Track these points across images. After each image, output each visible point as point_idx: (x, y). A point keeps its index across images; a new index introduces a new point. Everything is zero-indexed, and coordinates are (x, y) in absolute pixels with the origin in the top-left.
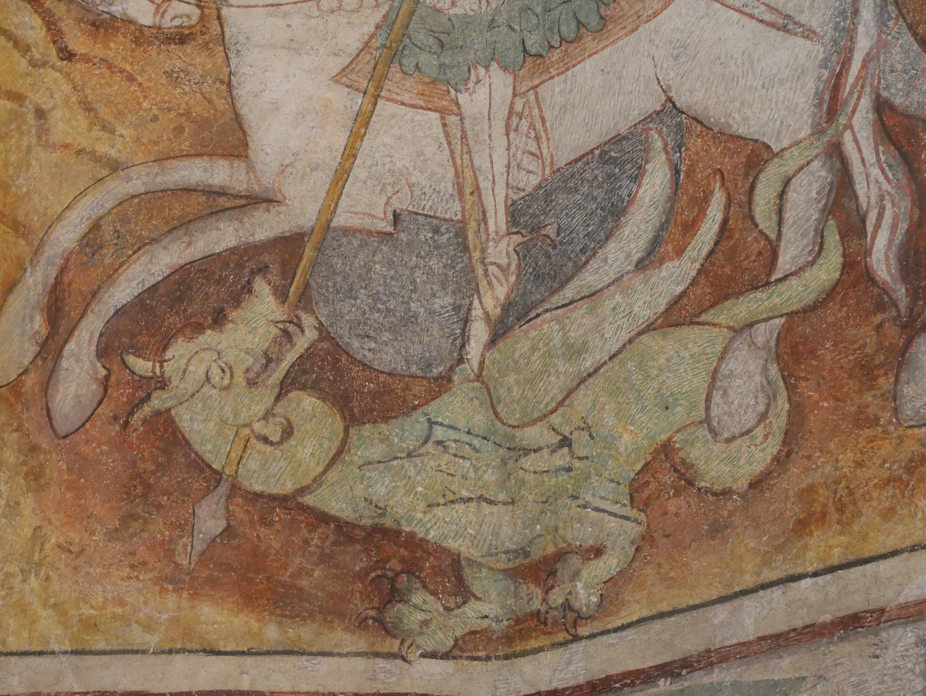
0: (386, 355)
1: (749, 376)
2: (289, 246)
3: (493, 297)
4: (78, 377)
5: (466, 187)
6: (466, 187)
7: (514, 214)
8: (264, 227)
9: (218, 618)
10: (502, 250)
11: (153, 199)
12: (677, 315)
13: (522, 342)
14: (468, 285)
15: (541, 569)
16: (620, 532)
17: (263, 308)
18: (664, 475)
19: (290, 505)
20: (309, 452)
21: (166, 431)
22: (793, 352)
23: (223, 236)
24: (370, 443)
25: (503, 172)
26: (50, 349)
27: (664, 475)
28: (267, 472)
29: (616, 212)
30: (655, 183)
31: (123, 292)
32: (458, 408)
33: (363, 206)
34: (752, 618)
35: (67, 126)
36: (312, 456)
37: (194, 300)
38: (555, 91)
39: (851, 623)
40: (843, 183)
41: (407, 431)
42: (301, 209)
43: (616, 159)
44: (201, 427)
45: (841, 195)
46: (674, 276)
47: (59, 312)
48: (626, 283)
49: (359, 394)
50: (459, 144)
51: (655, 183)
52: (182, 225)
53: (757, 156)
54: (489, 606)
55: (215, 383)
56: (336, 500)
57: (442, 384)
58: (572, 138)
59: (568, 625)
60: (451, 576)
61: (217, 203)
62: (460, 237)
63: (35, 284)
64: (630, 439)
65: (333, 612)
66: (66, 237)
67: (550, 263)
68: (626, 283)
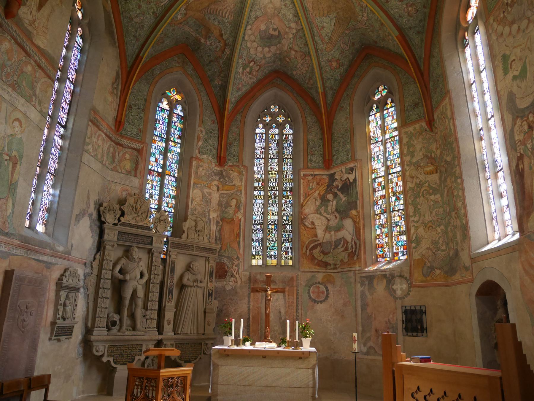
0: (326, 251)
1: (347, 256)
2: (320, 244)
3: (333, 247)
4: (308, 253)
5: (331, 239)
6: (331, 239)
7: (334, 242)
8: (319, 242)
9: (317, 267)
10: (333, 244)
11: (312, 240)
12: (343, 251)
13: (334, 251)
14: (331, 246)
15: (335, 265)
16: (340, 263)
17: (319, 248)
18: (342, 261)
19: (321, 261)
20: (322, 257)
21: (313, 256)
22: (349, 255)
23: (316, 243)
24: (325, 257)
25: (334, 239)
26: (306, 251)
27: (342, 261)
28: (319, 258)
29: (340, 243)
30: (342, 242)
31: (310, 247)
32: (331, 254)
33: (325, 241)
34: (346, 270)
35: (306, 235)
36: (321, 257)
37: (315, 247)
38: (337, 234)
39: (350, 271)
40: (352, 246)
41: (327, 256)
42: (321, 241)
43: (340, 240)
44: (315, 256)
45: (352, 246)
46: (343, 249)
47: (307, 248)
48: (340, 249)
49: (325, 253)
50: (331, 236)
51: (342, 242)
52: (314, 242)
53: (348, 242)
54: (332, 267)
55: (316, 252)
56: (323, 260)
57: (329, 253)
58: (338, 238)
59: (336, 268)
60: (330, 265)
61: (316, 241)
62: (331, 243)
63: (305, 246)
64: (340, 258)
65: (323, 267)
66: (307, 243)
67: (336, 246)
68: (340, 249)
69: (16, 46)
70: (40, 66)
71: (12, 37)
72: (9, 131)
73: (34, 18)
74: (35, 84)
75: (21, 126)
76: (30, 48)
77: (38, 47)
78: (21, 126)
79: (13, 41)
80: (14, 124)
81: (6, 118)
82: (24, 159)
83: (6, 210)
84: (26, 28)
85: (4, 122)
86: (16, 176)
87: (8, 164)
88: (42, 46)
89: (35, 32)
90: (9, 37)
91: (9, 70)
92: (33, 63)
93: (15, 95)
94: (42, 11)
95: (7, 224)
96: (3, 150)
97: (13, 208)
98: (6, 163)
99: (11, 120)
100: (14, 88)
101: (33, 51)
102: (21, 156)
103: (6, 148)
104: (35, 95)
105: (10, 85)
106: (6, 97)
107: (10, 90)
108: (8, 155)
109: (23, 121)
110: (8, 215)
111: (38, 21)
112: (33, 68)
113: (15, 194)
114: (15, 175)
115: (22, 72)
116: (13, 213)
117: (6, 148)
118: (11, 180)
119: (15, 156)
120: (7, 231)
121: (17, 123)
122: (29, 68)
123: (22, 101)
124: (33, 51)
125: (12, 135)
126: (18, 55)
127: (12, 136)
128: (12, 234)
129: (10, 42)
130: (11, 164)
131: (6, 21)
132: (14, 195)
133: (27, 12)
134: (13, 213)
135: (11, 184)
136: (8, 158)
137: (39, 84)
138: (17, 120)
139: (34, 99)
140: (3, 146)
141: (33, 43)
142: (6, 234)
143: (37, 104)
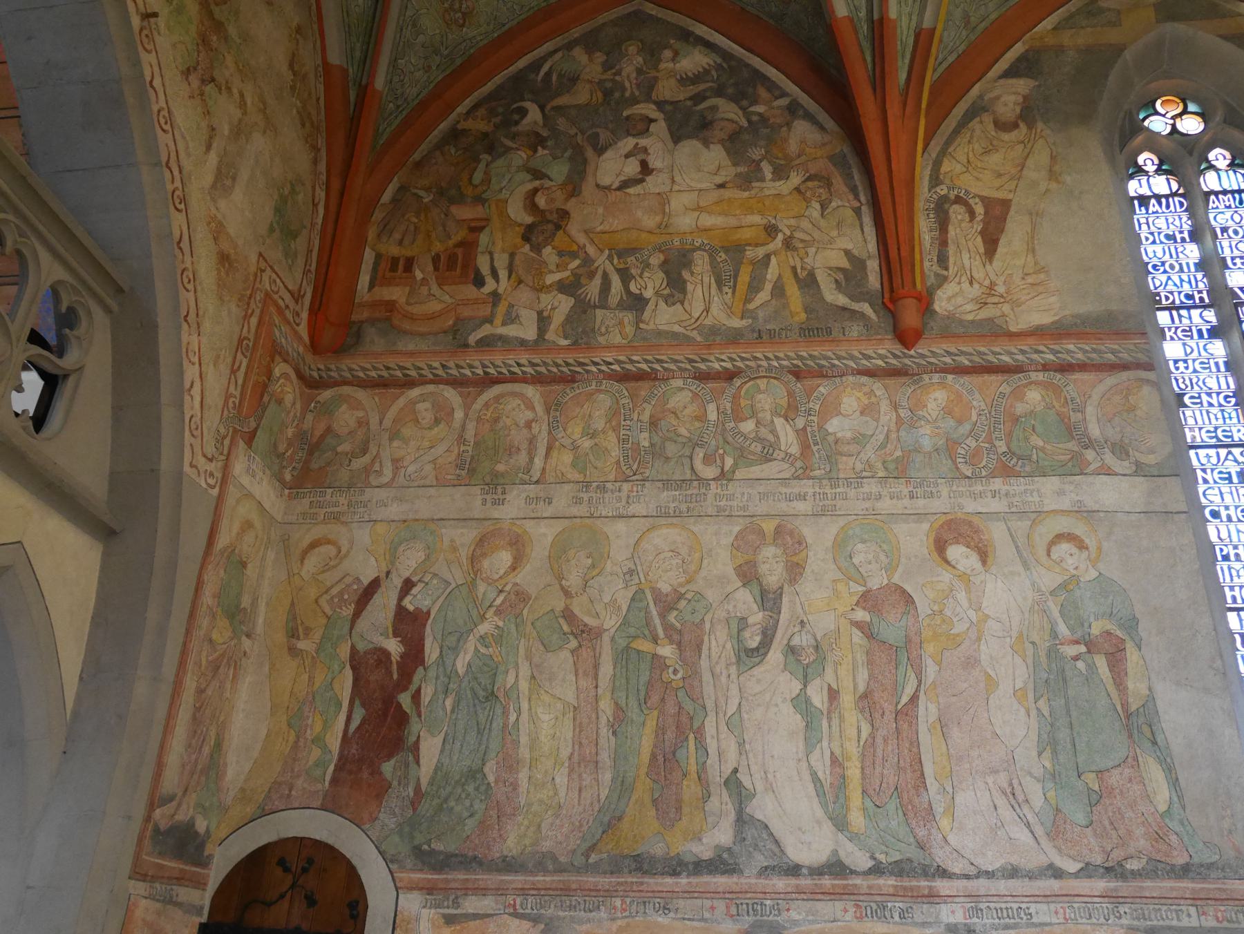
69: (965, 379)
70: (1065, 368)
71: (945, 370)
72: (1049, 580)
73: (987, 283)
74: (1075, 417)
75: (1082, 546)
76: (1010, 354)
77: (1038, 332)
78: (1082, 546)
79: (950, 377)
80: (1054, 556)
81: (1021, 556)
82: (1144, 628)
83: (1148, 797)
84: (973, 322)
85: (1020, 568)
86: (1136, 686)
87: (1092, 667)
88: (1046, 319)
89: (1006, 308)
90: (936, 378)
91: (973, 444)
92: (1040, 376)
93: (1017, 486)
94: (1001, 249)
95: (1174, 838)
96: (1054, 634)
97: (1174, 783)
98: (1080, 665)
99: (1041, 552)
100: (1007, 472)
101: (1023, 352)
102: (1131, 624)
103: (1063, 629)
104: (1089, 444)
105: (992, 475)
106: (996, 506)
107: (997, 484)
108: (1077, 642)
109: (1080, 530)
110: (1162, 808)
111: (1000, 281)
112: (1046, 386)
113: (1160, 738)
114: (1130, 685)
115: (1016, 420)
116: (1181, 798)
117: (1063, 629)
118: (1125, 705)
119: (1108, 633)
120: (1181, 860)
121: (1064, 547)
122: (1034, 396)
123: (1050, 484)
124: (1023, 352)
125: (1064, 586)
126: (978, 395)
127: (1067, 586)
128: (1210, 866)
129: (942, 385)
130: (1101, 662)
131: (912, 352)
132: (1155, 743)
133: (957, 289)
134: (1181, 798)
135: (1129, 716)
136: (1083, 649)
137: (1090, 410)
138: (1060, 537)
139: (1090, 455)
140: (1047, 627)
141: (1012, 336)
142: (1185, 871)
143: (1109, 459)
